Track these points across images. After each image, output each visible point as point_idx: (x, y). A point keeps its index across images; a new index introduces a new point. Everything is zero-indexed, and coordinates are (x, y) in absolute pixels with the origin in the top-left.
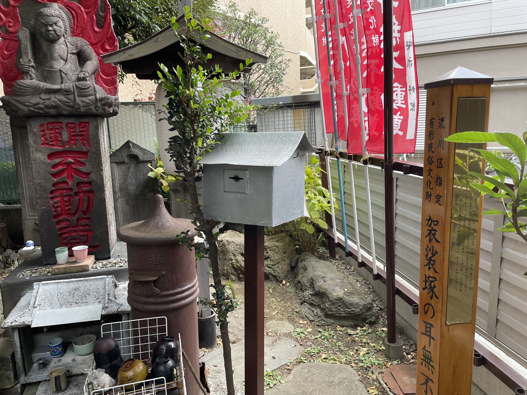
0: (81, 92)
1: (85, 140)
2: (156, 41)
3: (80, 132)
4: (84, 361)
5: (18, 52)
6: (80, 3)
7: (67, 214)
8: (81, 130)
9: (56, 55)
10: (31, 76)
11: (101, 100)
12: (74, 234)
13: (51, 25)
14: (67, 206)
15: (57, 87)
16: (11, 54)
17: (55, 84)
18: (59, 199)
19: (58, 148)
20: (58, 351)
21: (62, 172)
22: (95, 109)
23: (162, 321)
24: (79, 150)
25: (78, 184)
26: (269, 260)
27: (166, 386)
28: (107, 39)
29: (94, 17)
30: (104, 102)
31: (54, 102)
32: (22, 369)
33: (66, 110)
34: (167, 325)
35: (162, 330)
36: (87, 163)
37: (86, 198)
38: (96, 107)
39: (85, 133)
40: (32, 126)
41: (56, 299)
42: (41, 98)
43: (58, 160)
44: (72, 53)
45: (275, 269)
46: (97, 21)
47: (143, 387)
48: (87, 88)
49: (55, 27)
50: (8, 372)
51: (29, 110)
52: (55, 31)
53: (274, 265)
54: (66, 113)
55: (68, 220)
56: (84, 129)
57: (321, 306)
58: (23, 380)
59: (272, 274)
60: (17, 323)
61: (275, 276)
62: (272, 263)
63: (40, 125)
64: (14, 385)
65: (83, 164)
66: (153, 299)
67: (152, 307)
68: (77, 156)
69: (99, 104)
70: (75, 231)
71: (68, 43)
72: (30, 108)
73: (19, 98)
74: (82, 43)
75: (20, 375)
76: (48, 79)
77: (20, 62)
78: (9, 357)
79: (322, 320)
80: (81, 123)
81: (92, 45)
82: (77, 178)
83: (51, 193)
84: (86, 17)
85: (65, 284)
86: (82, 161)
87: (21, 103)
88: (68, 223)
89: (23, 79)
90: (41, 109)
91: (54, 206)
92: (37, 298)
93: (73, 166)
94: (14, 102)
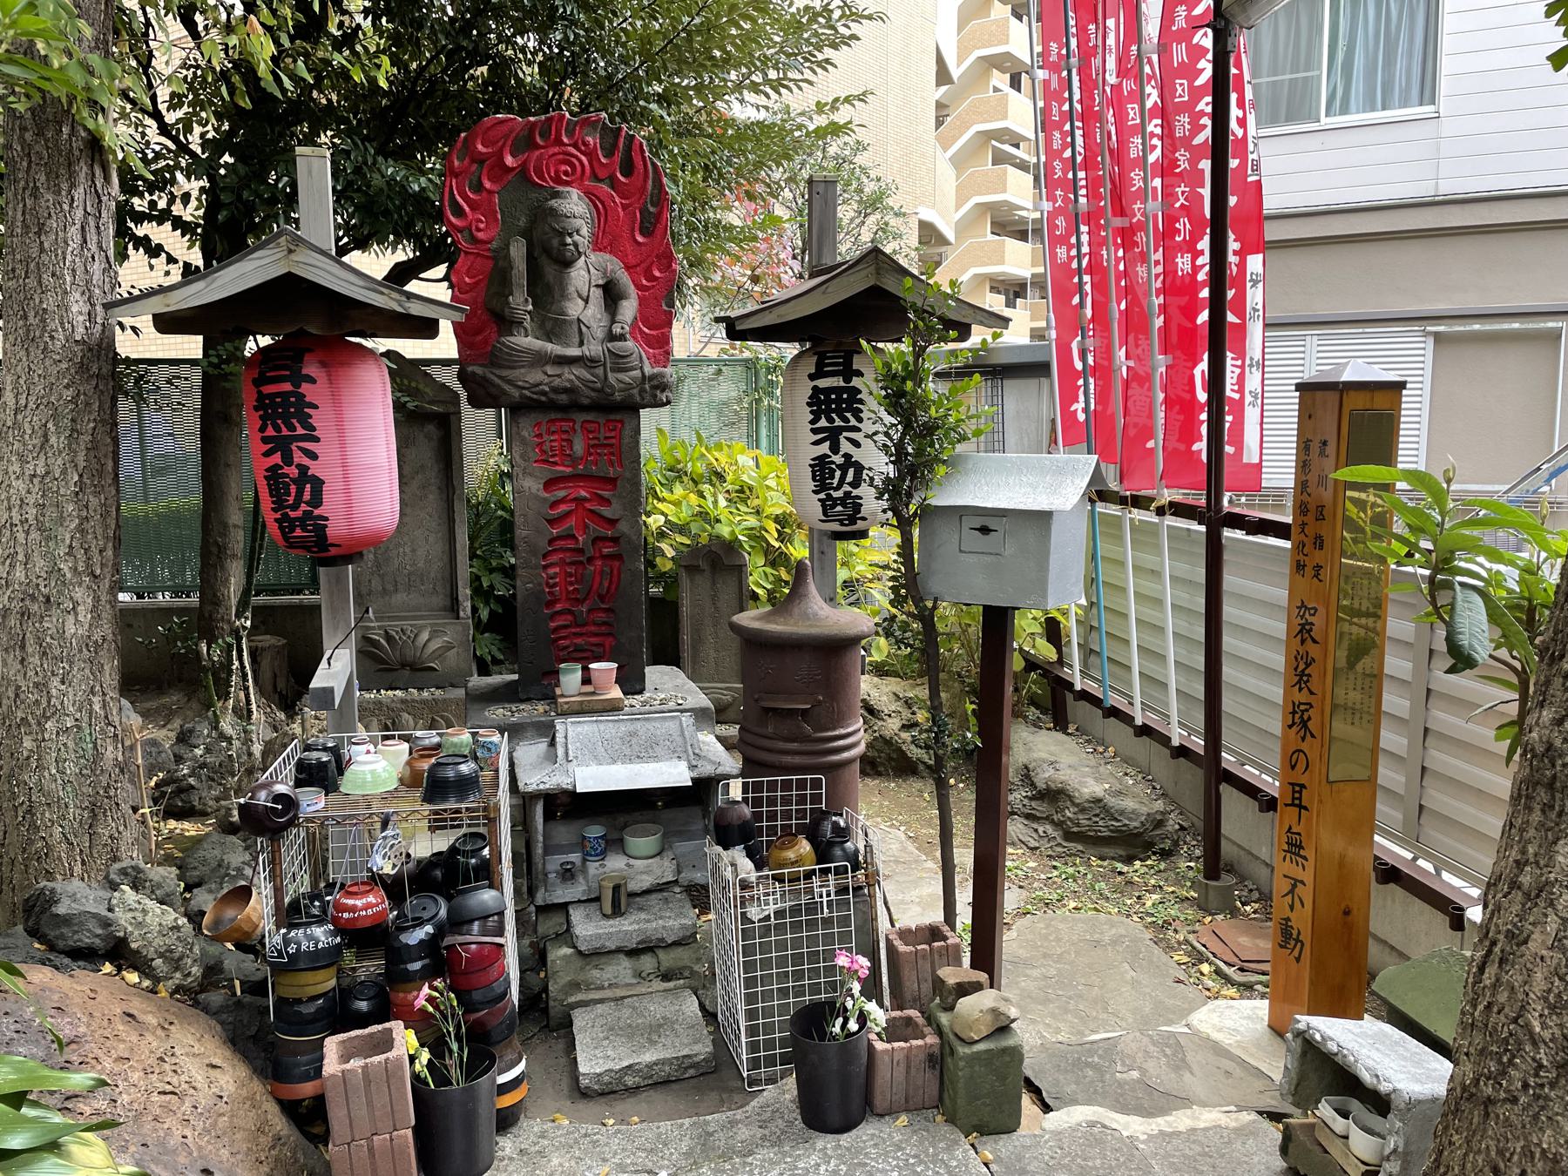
3: (606, 438)
6: (613, 188)
7: (568, 599)
9: (572, 289)
11: (653, 377)
12: (579, 641)
13: (570, 235)
14: (571, 584)
15: (574, 352)
16: (476, 283)
17: (568, 346)
18: (557, 570)
19: (561, 468)
21: (567, 515)
23: (816, 784)
24: (602, 474)
25: (596, 540)
28: (657, 256)
30: (655, 382)
31: (570, 381)
35: (816, 799)
36: (614, 501)
37: (607, 569)
38: (642, 391)
39: (614, 441)
42: (546, 374)
43: (562, 494)
44: (597, 286)
46: (642, 222)
49: (576, 237)
51: (522, 396)
52: (576, 245)
54: (586, 401)
55: (570, 612)
56: (613, 434)
57: (1055, 817)
59: (924, 763)
60: (547, 786)
65: (606, 502)
67: (797, 760)
69: (647, 386)
73: (505, 373)
76: (553, 334)
77: (508, 303)
78: (524, 851)
79: (1059, 845)
81: (628, 268)
83: (545, 557)
84: (622, 214)
85: (611, 725)
87: (510, 382)
89: (512, 335)
90: (544, 393)
91: (548, 584)
93: (588, 505)
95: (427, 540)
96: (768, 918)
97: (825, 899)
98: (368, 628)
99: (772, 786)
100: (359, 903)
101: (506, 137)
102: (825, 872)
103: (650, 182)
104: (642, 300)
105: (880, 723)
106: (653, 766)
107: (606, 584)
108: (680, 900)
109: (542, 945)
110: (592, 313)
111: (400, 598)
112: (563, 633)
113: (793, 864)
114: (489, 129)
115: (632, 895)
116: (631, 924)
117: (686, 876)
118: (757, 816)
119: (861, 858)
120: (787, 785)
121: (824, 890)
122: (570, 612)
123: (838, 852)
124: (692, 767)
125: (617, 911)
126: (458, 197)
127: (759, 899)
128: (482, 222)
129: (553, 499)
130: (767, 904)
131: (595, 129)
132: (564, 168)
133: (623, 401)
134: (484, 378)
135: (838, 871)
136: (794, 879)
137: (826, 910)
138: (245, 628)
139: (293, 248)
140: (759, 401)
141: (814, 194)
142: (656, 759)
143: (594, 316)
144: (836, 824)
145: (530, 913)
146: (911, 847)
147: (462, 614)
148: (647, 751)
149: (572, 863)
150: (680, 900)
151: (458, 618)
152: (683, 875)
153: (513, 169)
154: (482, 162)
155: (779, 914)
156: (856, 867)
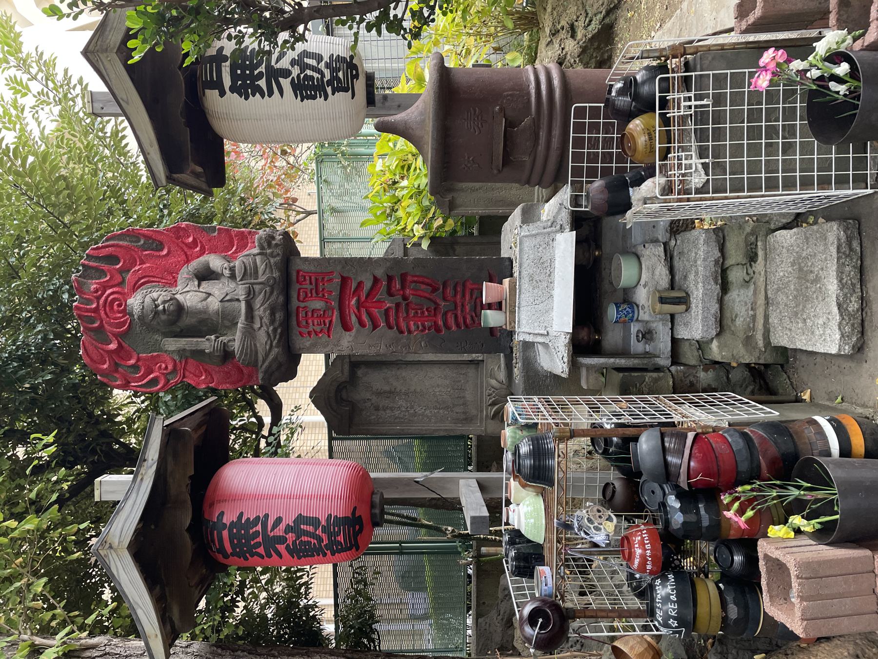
0: (251, 273)
1: (323, 279)
2: (127, 103)
4: (648, 268)
5: (198, 354)
6: (129, 271)
7: (435, 315)
8: (308, 282)
9: (200, 306)
10: (229, 341)
11: (262, 247)
12: (468, 308)
13: (157, 306)
14: (423, 313)
15: (243, 305)
16: (206, 371)
17: (240, 310)
18: (412, 323)
19: (334, 317)
20: (627, 309)
21: (370, 315)
22: (275, 257)
23: (580, 112)
24: (339, 288)
25: (390, 294)
26: (576, 23)
27: (673, 75)
28: (178, 238)
29: (146, 252)
30: (265, 245)
31: (265, 311)
32: (645, 361)
33: (277, 298)
34: (587, 105)
35: (595, 112)
36: (359, 279)
38: (272, 255)
39: (313, 278)
40: (302, 347)
41: (540, 307)
42: (260, 328)
43: (354, 318)
44: (199, 286)
45: (594, 10)
46: (152, 250)
47: (668, 115)
48: (245, 266)
49: (159, 301)
50: (647, 378)
51: (277, 347)
52: (164, 302)
53: (587, 14)
54: (281, 299)
55: (446, 313)
56: (307, 278)
58: (664, 361)
60: (566, 355)
61: (609, 12)
62: (582, 18)
63: (301, 338)
64: (669, 374)
65: (360, 284)
66: (541, 130)
67: (556, 132)
68: (348, 292)
69: (269, 251)
70: (463, 305)
71: (184, 290)
72: (274, 345)
73: (260, 358)
74: (184, 273)
75: (655, 364)
78: (621, 375)
80: (298, 282)
81: (188, 261)
82: (381, 294)
83: (402, 332)
84: (148, 265)
85: (522, 296)
86: (356, 285)
87: (267, 355)
88: (449, 314)
89: (234, 351)
90: (275, 330)
91: (422, 331)
92: (536, 332)
93: (363, 298)
94: (266, 364)
95: (432, 378)
96: (705, 166)
97: (693, 103)
98: (487, 416)
99: (578, 157)
100: (638, 551)
101: (96, 347)
102: (664, 103)
103: (121, 243)
104: (213, 251)
105: (568, 57)
106: (557, 264)
107: (423, 287)
108: (683, 241)
109: (707, 362)
110: (217, 290)
111: (469, 396)
112: (461, 320)
113: (651, 138)
114: (92, 360)
115: (672, 286)
116: (697, 289)
117: (662, 235)
118: (606, 172)
119: (655, 63)
120: (578, 143)
121: (683, 104)
122: (446, 313)
123: (645, 89)
124: (562, 229)
125: (684, 301)
126: (143, 382)
127: (683, 175)
128: (160, 366)
129: (357, 325)
130: (690, 167)
131: (85, 283)
132: (115, 307)
133: (280, 271)
134: (266, 372)
135: (666, 87)
136: (668, 137)
137: (705, 102)
138: (453, 531)
139: (107, 545)
140: (343, 154)
141: (103, 111)
142: (552, 260)
143: (220, 289)
144: (621, 92)
145: (677, 371)
146: (668, 25)
147: (480, 358)
148: (546, 267)
149: (638, 331)
150: (683, 241)
151: (483, 361)
152: (660, 238)
153: (119, 343)
154: (116, 364)
155: (702, 153)
156: (663, 68)
